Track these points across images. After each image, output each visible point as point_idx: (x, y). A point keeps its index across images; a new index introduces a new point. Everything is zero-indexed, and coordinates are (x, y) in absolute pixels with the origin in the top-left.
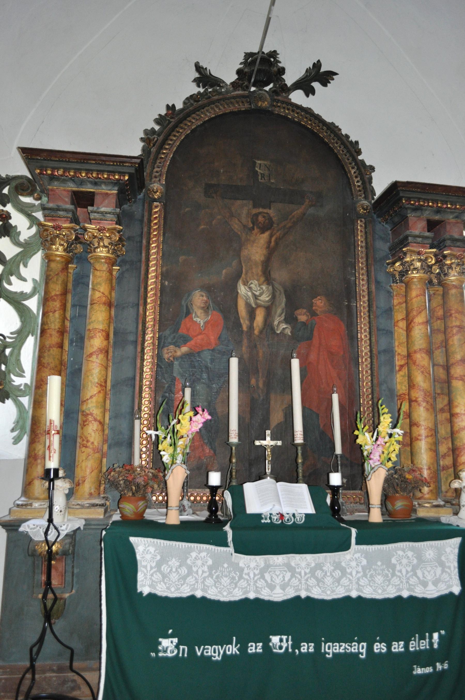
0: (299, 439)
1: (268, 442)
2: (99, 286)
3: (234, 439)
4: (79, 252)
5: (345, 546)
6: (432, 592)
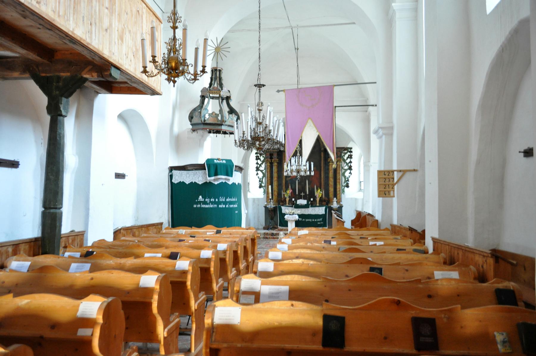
1: (302, 194)
2: (275, 169)
3: (297, 193)
4: (271, 163)
5: (309, 207)
6: (321, 214)
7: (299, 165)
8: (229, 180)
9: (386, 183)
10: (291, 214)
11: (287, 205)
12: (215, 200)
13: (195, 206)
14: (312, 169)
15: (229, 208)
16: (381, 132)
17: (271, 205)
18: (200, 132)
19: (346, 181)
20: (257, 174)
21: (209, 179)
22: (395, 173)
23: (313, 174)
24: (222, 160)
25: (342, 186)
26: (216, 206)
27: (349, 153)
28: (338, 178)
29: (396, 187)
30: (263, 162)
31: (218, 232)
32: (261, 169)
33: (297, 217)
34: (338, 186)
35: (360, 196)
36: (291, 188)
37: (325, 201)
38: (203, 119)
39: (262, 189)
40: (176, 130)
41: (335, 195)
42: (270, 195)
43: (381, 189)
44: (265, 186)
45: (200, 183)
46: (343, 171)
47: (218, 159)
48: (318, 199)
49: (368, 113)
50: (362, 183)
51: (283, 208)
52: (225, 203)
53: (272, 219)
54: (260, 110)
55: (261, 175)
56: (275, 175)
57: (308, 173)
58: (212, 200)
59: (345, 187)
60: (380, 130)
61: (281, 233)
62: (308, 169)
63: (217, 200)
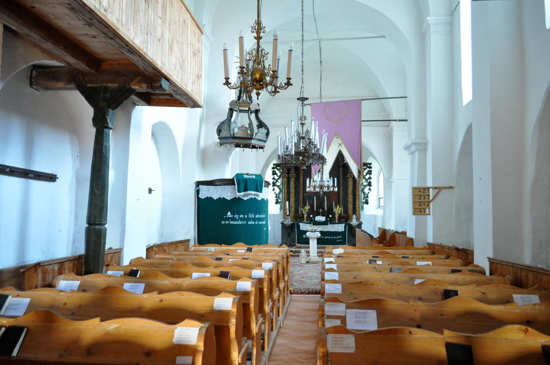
0: (326, 209)
1: (321, 210)
2: (292, 184)
3: (315, 210)
4: (289, 179)
6: (340, 231)
7: (322, 180)
8: (258, 195)
9: (421, 200)
10: (313, 232)
11: (305, 221)
12: (244, 216)
13: (223, 222)
14: (336, 185)
15: (258, 224)
16: (414, 148)
17: (288, 222)
18: (228, 146)
19: (365, 197)
20: (274, 189)
21: (238, 194)
22: (431, 190)
23: (336, 189)
24: (252, 175)
25: (361, 202)
26: (245, 222)
27: (368, 169)
28: (357, 194)
29: (431, 204)
30: (280, 177)
31: (250, 250)
32: (278, 184)
33: (319, 235)
34: (357, 203)
35: (380, 212)
36: (309, 205)
37: (344, 217)
38: (232, 133)
39: (279, 205)
40: (202, 144)
41: (354, 212)
42: (288, 211)
43: (416, 207)
44: (282, 202)
45: (229, 199)
46: (362, 187)
47: (247, 174)
48: (337, 216)
49: (389, 128)
50: (382, 200)
51: (301, 224)
52: (254, 219)
53: (289, 236)
54: (303, 124)
55: (277, 190)
56: (292, 191)
57: (331, 189)
58: (241, 216)
59: (364, 203)
60: (413, 146)
61: (303, 250)
62: (332, 185)
63: (246, 216)
